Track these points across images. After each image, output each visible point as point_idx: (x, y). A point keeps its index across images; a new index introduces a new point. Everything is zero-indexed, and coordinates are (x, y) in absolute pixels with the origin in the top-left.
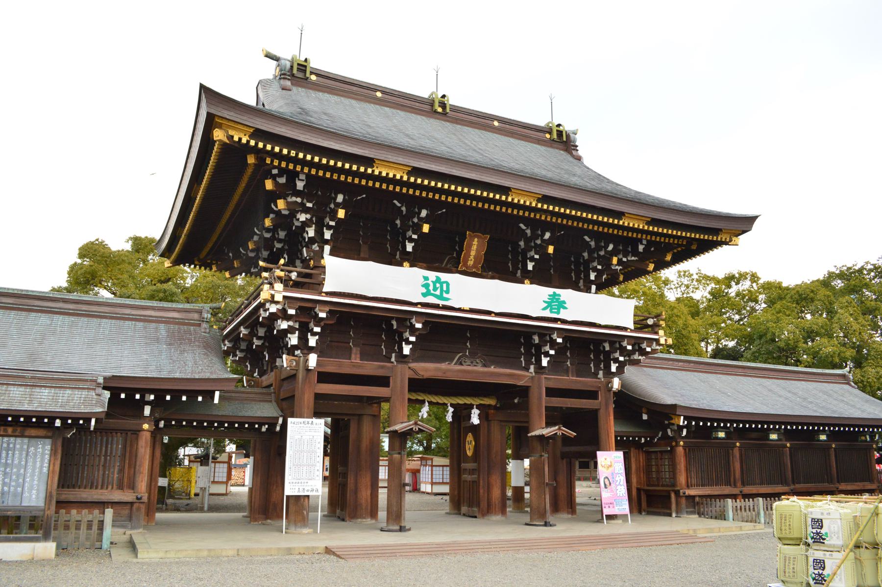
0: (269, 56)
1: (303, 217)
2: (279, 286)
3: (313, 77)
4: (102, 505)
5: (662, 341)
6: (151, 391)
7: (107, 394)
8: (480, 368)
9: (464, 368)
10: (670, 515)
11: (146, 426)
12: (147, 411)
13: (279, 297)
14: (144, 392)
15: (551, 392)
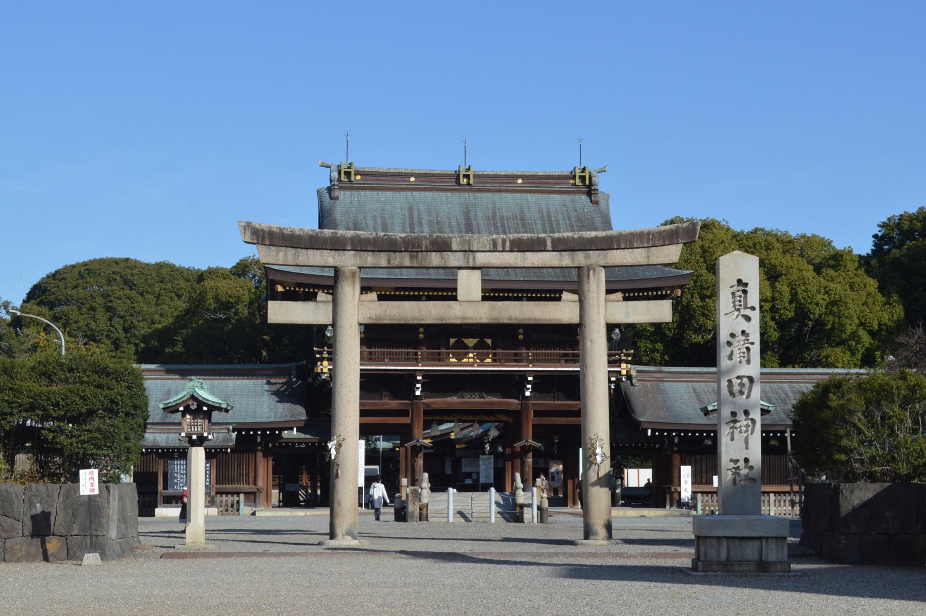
2: (325, 363)
3: (358, 177)
4: (238, 494)
5: (624, 372)
6: (259, 429)
7: (234, 435)
8: (477, 400)
9: (466, 400)
10: (665, 507)
12: (259, 439)
13: (325, 370)
14: (255, 430)
15: (537, 414)
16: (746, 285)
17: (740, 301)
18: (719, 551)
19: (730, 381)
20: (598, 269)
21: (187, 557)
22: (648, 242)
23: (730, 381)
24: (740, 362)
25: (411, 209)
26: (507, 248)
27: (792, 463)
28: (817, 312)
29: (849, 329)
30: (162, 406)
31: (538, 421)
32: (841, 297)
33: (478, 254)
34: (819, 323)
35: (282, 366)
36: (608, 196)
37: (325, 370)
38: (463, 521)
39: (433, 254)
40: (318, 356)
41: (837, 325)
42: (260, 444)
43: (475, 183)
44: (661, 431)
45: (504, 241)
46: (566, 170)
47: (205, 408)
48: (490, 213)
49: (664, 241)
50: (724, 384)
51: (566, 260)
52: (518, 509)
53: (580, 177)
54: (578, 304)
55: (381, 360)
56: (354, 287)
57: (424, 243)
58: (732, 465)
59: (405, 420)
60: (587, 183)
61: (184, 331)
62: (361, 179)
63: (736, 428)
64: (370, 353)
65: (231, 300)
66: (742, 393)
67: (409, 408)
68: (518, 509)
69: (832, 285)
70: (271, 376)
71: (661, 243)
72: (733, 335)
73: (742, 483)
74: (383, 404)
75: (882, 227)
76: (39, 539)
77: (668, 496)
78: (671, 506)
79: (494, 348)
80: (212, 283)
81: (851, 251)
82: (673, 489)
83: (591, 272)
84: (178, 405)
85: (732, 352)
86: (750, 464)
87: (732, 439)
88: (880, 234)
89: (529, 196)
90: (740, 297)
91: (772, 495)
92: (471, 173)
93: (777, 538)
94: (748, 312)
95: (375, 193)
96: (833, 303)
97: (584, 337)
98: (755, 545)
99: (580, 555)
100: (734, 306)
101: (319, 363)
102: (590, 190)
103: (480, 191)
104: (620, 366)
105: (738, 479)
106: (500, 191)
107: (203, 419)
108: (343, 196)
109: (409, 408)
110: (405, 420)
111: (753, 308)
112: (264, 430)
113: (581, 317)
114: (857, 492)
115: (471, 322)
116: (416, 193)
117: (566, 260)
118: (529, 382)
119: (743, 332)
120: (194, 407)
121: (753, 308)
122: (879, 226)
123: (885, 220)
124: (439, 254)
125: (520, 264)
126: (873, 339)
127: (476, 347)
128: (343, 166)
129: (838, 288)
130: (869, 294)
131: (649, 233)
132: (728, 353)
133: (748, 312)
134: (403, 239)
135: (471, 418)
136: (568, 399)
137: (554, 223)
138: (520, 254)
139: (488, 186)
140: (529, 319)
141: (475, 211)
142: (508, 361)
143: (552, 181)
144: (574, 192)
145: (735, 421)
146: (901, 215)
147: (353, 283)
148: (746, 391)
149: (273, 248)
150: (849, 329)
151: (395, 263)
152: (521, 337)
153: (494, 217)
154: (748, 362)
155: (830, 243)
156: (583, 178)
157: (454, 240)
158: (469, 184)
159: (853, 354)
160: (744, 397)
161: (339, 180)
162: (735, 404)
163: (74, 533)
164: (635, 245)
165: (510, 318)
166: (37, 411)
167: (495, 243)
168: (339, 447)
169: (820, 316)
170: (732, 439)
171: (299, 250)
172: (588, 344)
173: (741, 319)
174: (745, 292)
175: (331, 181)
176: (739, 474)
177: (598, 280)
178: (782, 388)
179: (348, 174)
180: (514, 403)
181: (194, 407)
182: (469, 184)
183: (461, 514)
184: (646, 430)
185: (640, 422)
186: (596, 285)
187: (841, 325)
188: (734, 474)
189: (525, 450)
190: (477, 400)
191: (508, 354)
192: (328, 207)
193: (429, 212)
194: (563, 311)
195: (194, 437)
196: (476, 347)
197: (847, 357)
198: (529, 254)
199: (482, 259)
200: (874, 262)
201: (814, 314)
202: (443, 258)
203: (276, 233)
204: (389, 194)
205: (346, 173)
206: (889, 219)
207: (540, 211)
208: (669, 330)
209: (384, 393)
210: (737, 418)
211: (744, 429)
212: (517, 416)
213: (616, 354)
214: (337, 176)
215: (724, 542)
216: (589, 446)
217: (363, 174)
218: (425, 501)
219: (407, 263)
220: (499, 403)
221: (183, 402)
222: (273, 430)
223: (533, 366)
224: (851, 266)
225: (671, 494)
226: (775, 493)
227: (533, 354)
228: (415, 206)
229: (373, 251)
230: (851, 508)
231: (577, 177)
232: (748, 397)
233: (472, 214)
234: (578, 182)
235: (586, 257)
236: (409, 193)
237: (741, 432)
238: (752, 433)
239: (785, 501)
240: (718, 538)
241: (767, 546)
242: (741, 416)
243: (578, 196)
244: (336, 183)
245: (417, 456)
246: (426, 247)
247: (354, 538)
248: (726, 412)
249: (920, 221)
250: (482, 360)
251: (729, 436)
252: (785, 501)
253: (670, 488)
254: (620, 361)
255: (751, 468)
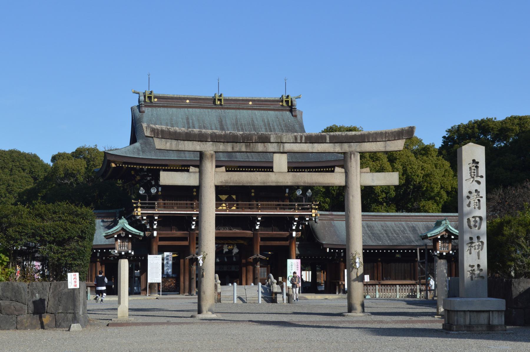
0: (134, 93)
1: (149, 178)
2: (139, 209)
3: (156, 100)
5: (314, 215)
8: (228, 231)
9: (221, 231)
11: (98, 260)
12: (98, 255)
13: (139, 214)
15: (263, 239)
16: (478, 163)
17: (474, 172)
18: (465, 319)
19: (468, 219)
20: (356, 153)
21: (140, 325)
22: (386, 138)
23: (468, 219)
24: (475, 208)
25: (187, 119)
26: (303, 141)
27: (420, 267)
28: (418, 181)
29: (436, 190)
30: (104, 235)
31: (262, 243)
32: (431, 172)
33: (286, 144)
34: (418, 187)
35: (110, 211)
36: (302, 112)
37: (139, 214)
38: (241, 302)
39: (260, 144)
40: (135, 205)
41: (429, 188)
42: (99, 258)
43: (224, 103)
44: (335, 249)
45: (301, 137)
46: (277, 96)
47: (130, 236)
48: (234, 122)
49: (395, 137)
50: (465, 221)
51: (337, 148)
52: (274, 295)
53: (286, 101)
54: (344, 174)
55: (172, 208)
56: (212, 163)
57: (254, 137)
58: (470, 269)
59: (186, 243)
60: (290, 105)
61: (44, 191)
62: (158, 101)
63: (472, 247)
64: (165, 204)
65: (74, 172)
66: (475, 226)
67: (188, 236)
68: (274, 295)
69: (425, 165)
70: (104, 217)
71: (393, 139)
72: (470, 192)
73: (476, 279)
74: (172, 234)
75: (448, 132)
76: (38, 316)
77: (337, 287)
78: (339, 293)
79: (237, 201)
80: (62, 162)
81: (434, 146)
82: (340, 283)
83: (352, 155)
84: (114, 234)
85: (470, 202)
86: (481, 268)
87: (470, 253)
88: (447, 136)
89: (256, 112)
90: (474, 170)
91: (398, 286)
92: (222, 98)
93: (498, 311)
94: (479, 179)
95: (166, 109)
96: (427, 175)
97: (348, 194)
98: (485, 315)
99: (349, 322)
100: (471, 175)
101: (135, 210)
102: (292, 108)
103: (228, 108)
104: (311, 212)
105: (474, 276)
106: (239, 109)
107: (128, 242)
108: (147, 111)
109: (188, 236)
110: (186, 243)
111: (482, 177)
112: (102, 249)
113: (346, 182)
114: (522, 284)
115: (281, 184)
116: (190, 110)
117: (337, 148)
118: (258, 221)
119: (476, 191)
120: (123, 235)
121: (482, 177)
122: (447, 131)
123: (450, 128)
124: (263, 144)
125: (311, 151)
126: (448, 196)
127: (226, 200)
128: (147, 93)
129: (429, 167)
130: (446, 170)
131: (386, 133)
132: (467, 203)
133: (479, 179)
134: (242, 135)
135: (222, 242)
136: (280, 230)
137: (272, 127)
138: (310, 144)
139: (232, 106)
140: (316, 183)
141: (226, 121)
142: (246, 208)
143: (269, 103)
144: (282, 110)
145: (472, 243)
146: (459, 125)
147: (212, 161)
148: (477, 224)
149: (163, 140)
150: (436, 190)
151: (237, 149)
152: (253, 194)
153: (237, 124)
154: (479, 208)
155: (421, 141)
156: (287, 102)
157: (272, 136)
158: (221, 104)
159: (438, 205)
160: (477, 228)
161: (145, 101)
162: (472, 233)
163: (60, 311)
164: (378, 140)
165: (305, 182)
166: (37, 238)
167: (296, 138)
168: (204, 258)
169: (419, 183)
170: (470, 253)
171: (179, 141)
172: (351, 198)
173: (476, 183)
174: (477, 167)
175: (139, 102)
176: (474, 274)
177: (356, 161)
178: (401, 224)
179: (150, 98)
180: (249, 233)
181: (123, 235)
182: (221, 104)
183: (240, 298)
184: (326, 249)
185: (322, 244)
186: (355, 163)
187: (432, 188)
188: (471, 273)
189: (256, 260)
190: (228, 231)
191: (246, 204)
192: (138, 117)
193: (198, 120)
194: (336, 178)
195: (123, 253)
196: (226, 200)
197: (435, 206)
198: (316, 145)
199: (288, 147)
200: (444, 152)
201: (416, 182)
202: (265, 146)
203: (165, 131)
204: (174, 110)
205: (148, 97)
206: (452, 128)
207: (263, 121)
208: (334, 190)
209: (173, 227)
210: (473, 241)
211: (477, 247)
212: (250, 241)
213: (308, 205)
214: (143, 99)
215: (468, 314)
216: (351, 258)
217: (158, 98)
218: (219, 291)
219: (244, 149)
220: (240, 233)
221: (117, 232)
222: (107, 249)
223: (261, 211)
224: (435, 154)
225: (339, 285)
226: (399, 285)
227: (262, 205)
228: (190, 117)
229: (224, 142)
230: (518, 293)
231: (284, 101)
232: (479, 228)
233: (224, 122)
234: (285, 104)
235: (349, 147)
236: (186, 109)
237: (475, 249)
238: (481, 250)
239: (405, 290)
240: (464, 311)
241: (493, 316)
242: (475, 240)
243: (284, 112)
244: (143, 103)
245: (193, 264)
246: (256, 140)
247: (213, 313)
248: (466, 237)
249: (471, 129)
250: (230, 208)
251: (469, 251)
252: (405, 290)
253: (339, 283)
254: (312, 208)
255: (481, 270)
